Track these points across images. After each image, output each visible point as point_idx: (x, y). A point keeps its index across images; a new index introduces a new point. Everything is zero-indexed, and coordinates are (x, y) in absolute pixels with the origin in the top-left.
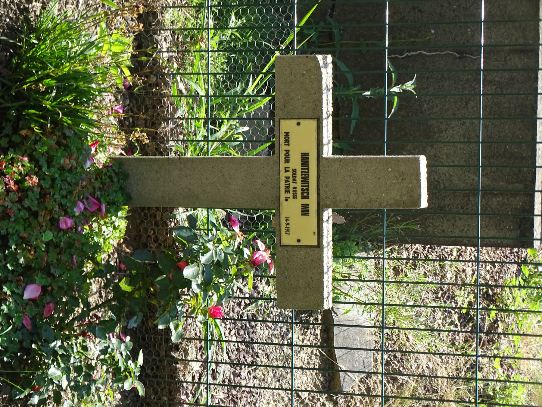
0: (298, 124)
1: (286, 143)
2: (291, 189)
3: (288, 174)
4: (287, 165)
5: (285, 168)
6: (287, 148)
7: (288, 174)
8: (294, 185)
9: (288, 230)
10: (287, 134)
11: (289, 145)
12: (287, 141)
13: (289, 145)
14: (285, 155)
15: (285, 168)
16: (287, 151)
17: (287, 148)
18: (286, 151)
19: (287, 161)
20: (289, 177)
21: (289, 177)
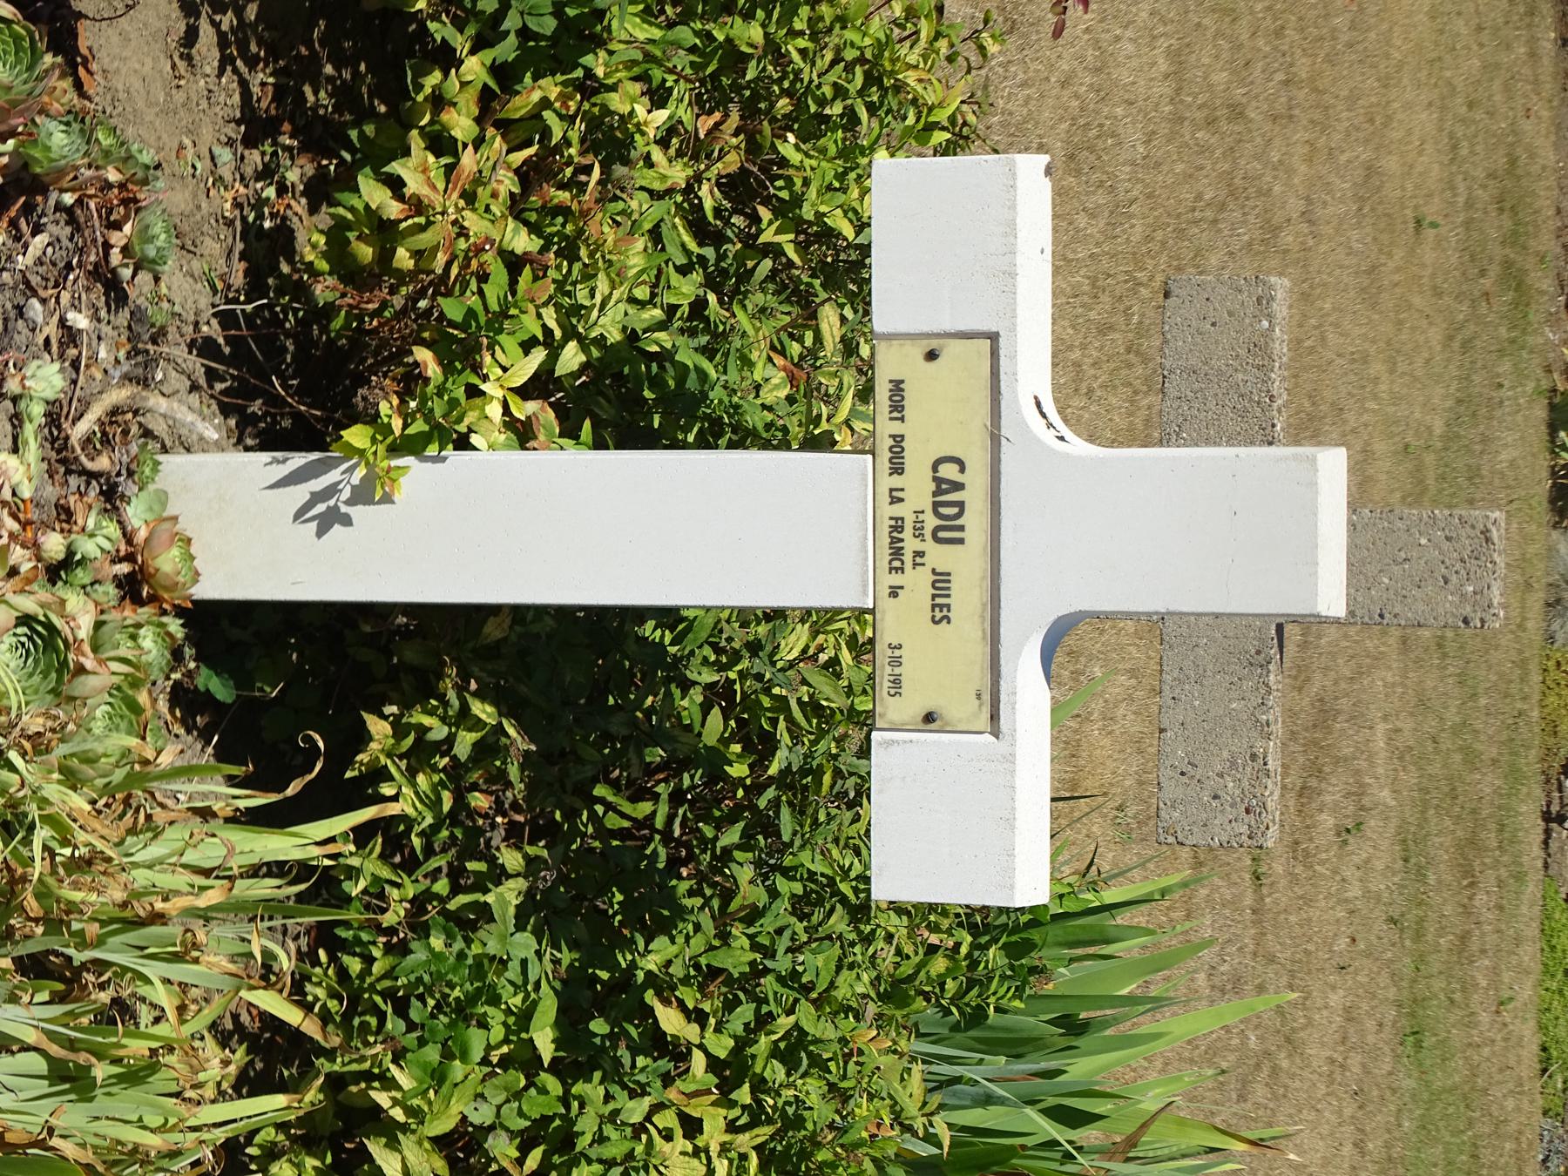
0: (931, 356)
1: (895, 414)
2: (908, 558)
3: (897, 511)
4: (896, 481)
5: (891, 490)
6: (896, 428)
7: (897, 511)
8: (917, 545)
9: (896, 682)
10: (897, 386)
11: (902, 419)
12: (897, 407)
13: (902, 419)
14: (891, 448)
15: (891, 490)
16: (898, 439)
17: (896, 428)
18: (893, 437)
19: (897, 469)
20: (902, 519)
21: (902, 519)
